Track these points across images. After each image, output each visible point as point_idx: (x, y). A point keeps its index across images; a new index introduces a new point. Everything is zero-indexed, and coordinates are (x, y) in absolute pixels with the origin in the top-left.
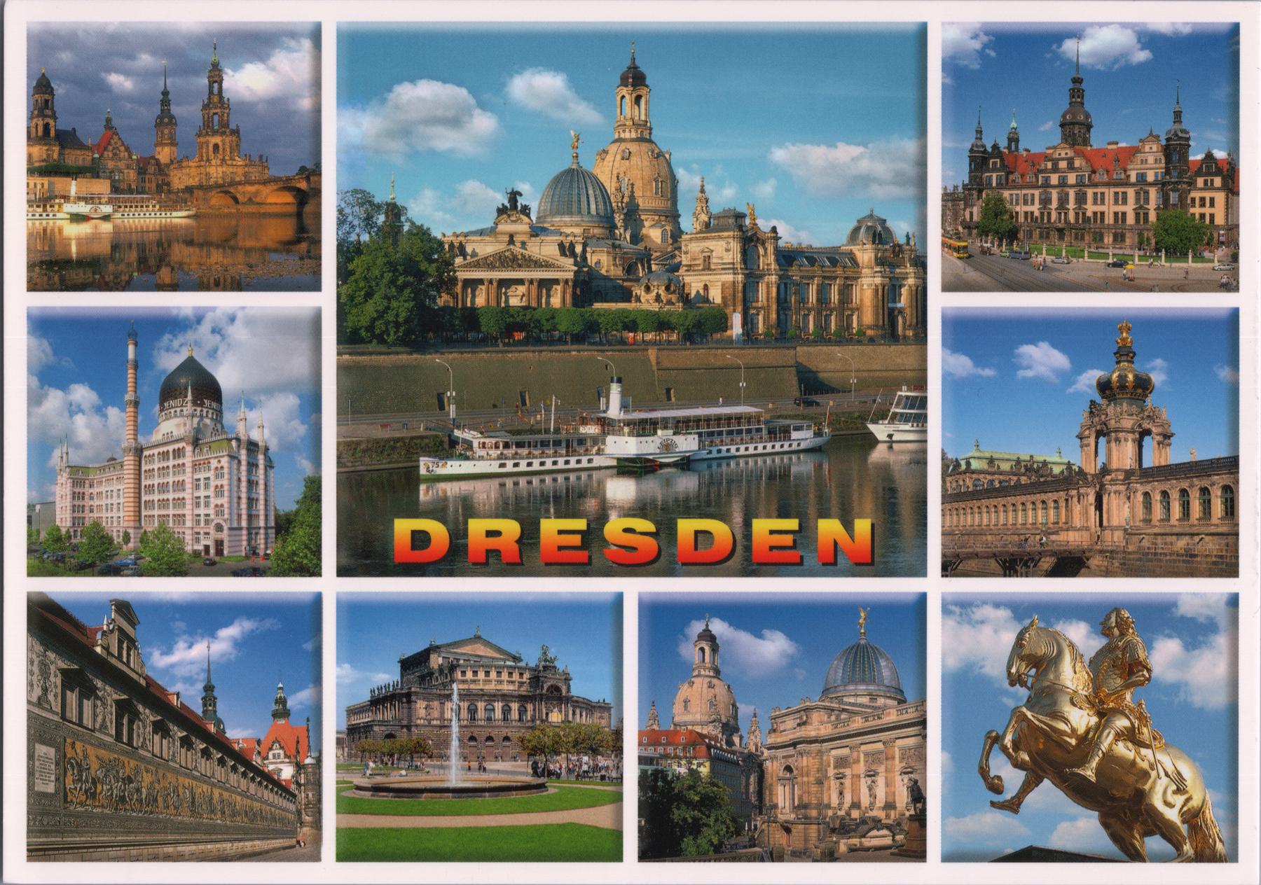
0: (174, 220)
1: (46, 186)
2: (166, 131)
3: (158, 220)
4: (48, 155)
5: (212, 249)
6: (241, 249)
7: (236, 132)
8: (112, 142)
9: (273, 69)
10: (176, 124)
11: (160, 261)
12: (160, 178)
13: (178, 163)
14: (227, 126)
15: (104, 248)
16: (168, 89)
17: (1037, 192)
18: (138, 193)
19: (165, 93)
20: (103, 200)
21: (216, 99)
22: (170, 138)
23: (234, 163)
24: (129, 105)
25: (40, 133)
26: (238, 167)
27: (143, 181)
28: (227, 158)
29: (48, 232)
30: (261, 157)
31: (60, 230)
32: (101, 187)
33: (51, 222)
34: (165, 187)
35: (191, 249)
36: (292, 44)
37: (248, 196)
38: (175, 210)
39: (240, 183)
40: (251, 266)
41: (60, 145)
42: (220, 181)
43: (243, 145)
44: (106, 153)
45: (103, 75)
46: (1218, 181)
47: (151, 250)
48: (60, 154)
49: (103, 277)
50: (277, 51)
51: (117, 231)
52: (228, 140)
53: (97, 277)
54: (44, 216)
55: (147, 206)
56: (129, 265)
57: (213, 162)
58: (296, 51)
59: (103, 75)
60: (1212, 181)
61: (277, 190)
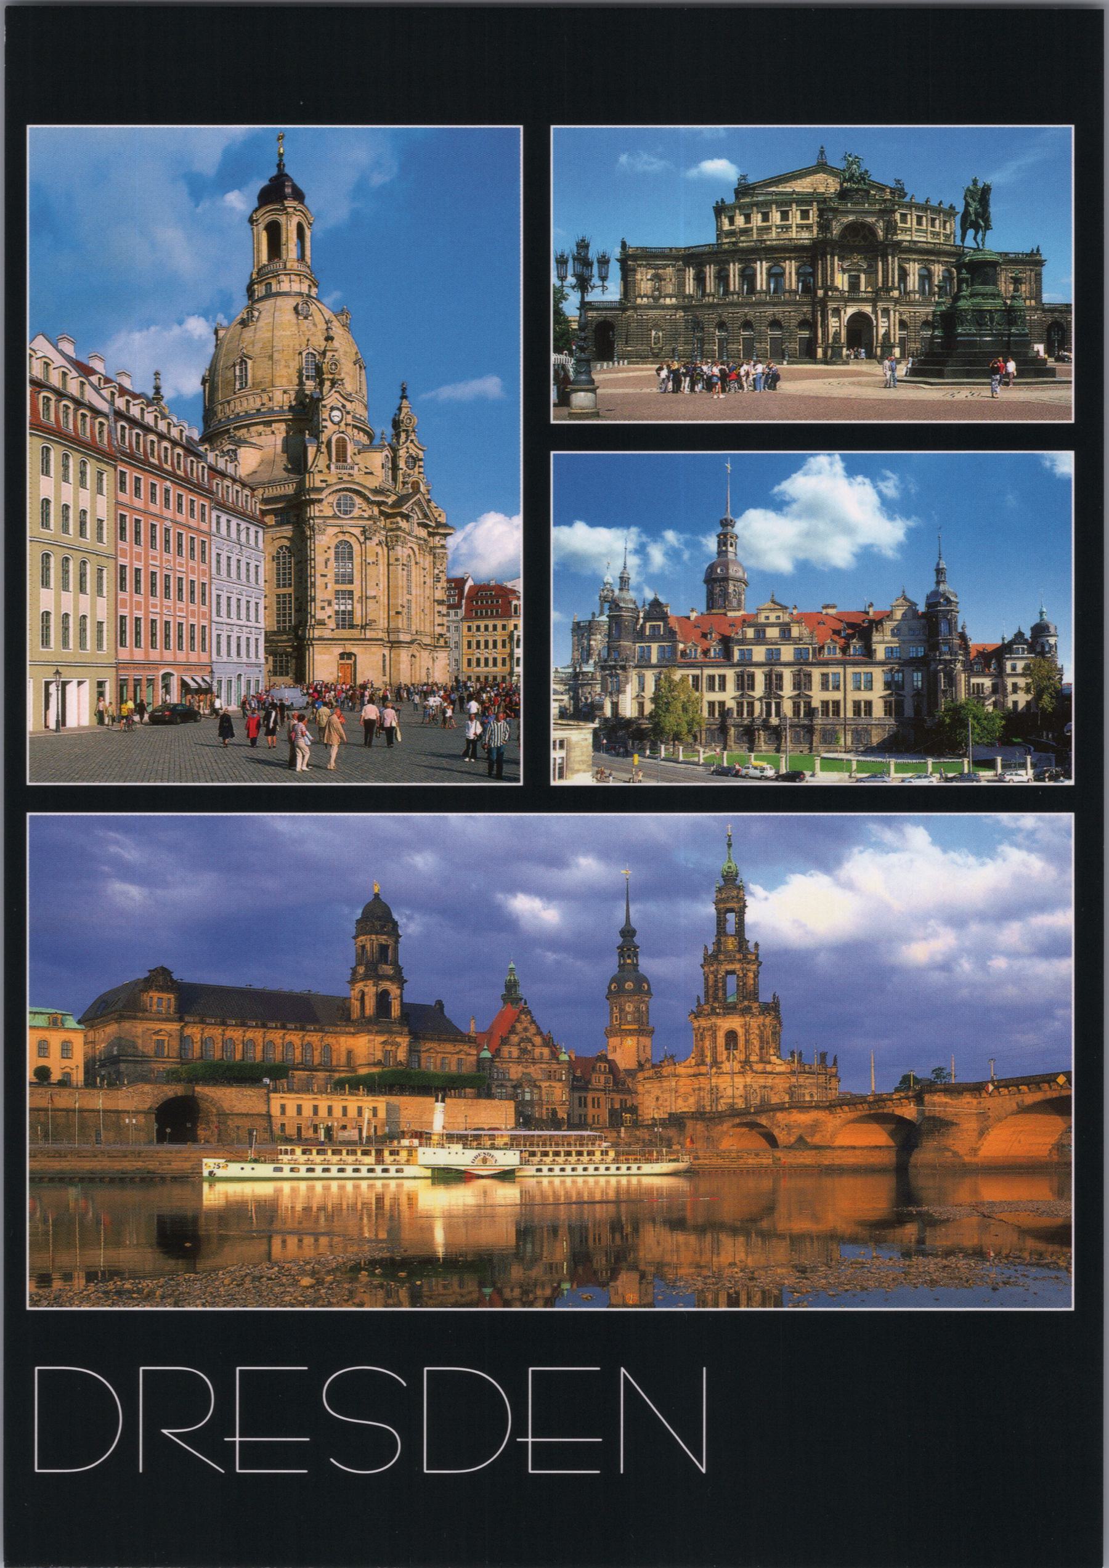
0: (646, 1181)
2: (629, 1008)
3: (613, 1180)
4: (386, 1053)
6: (781, 1237)
8: (519, 1027)
9: (849, 886)
10: (649, 993)
11: (618, 1259)
12: (617, 1097)
14: (754, 995)
16: (634, 924)
18: (571, 1127)
19: (628, 933)
20: (499, 1142)
21: (731, 944)
23: (769, 1068)
24: (551, 957)
27: (582, 1103)
28: (754, 1058)
29: (387, 1202)
30: (823, 1056)
31: (412, 1199)
33: (393, 1184)
35: (680, 1237)
36: (888, 836)
37: (797, 1132)
38: (649, 1161)
39: (780, 1108)
40: (803, 1271)
41: (411, 1033)
42: (740, 1104)
44: (505, 1049)
45: (500, 897)
48: (412, 1051)
50: (856, 850)
51: (527, 1202)
52: (754, 1022)
55: (591, 1153)
56: (551, 1267)
57: (726, 1067)
58: (895, 850)
59: (500, 897)
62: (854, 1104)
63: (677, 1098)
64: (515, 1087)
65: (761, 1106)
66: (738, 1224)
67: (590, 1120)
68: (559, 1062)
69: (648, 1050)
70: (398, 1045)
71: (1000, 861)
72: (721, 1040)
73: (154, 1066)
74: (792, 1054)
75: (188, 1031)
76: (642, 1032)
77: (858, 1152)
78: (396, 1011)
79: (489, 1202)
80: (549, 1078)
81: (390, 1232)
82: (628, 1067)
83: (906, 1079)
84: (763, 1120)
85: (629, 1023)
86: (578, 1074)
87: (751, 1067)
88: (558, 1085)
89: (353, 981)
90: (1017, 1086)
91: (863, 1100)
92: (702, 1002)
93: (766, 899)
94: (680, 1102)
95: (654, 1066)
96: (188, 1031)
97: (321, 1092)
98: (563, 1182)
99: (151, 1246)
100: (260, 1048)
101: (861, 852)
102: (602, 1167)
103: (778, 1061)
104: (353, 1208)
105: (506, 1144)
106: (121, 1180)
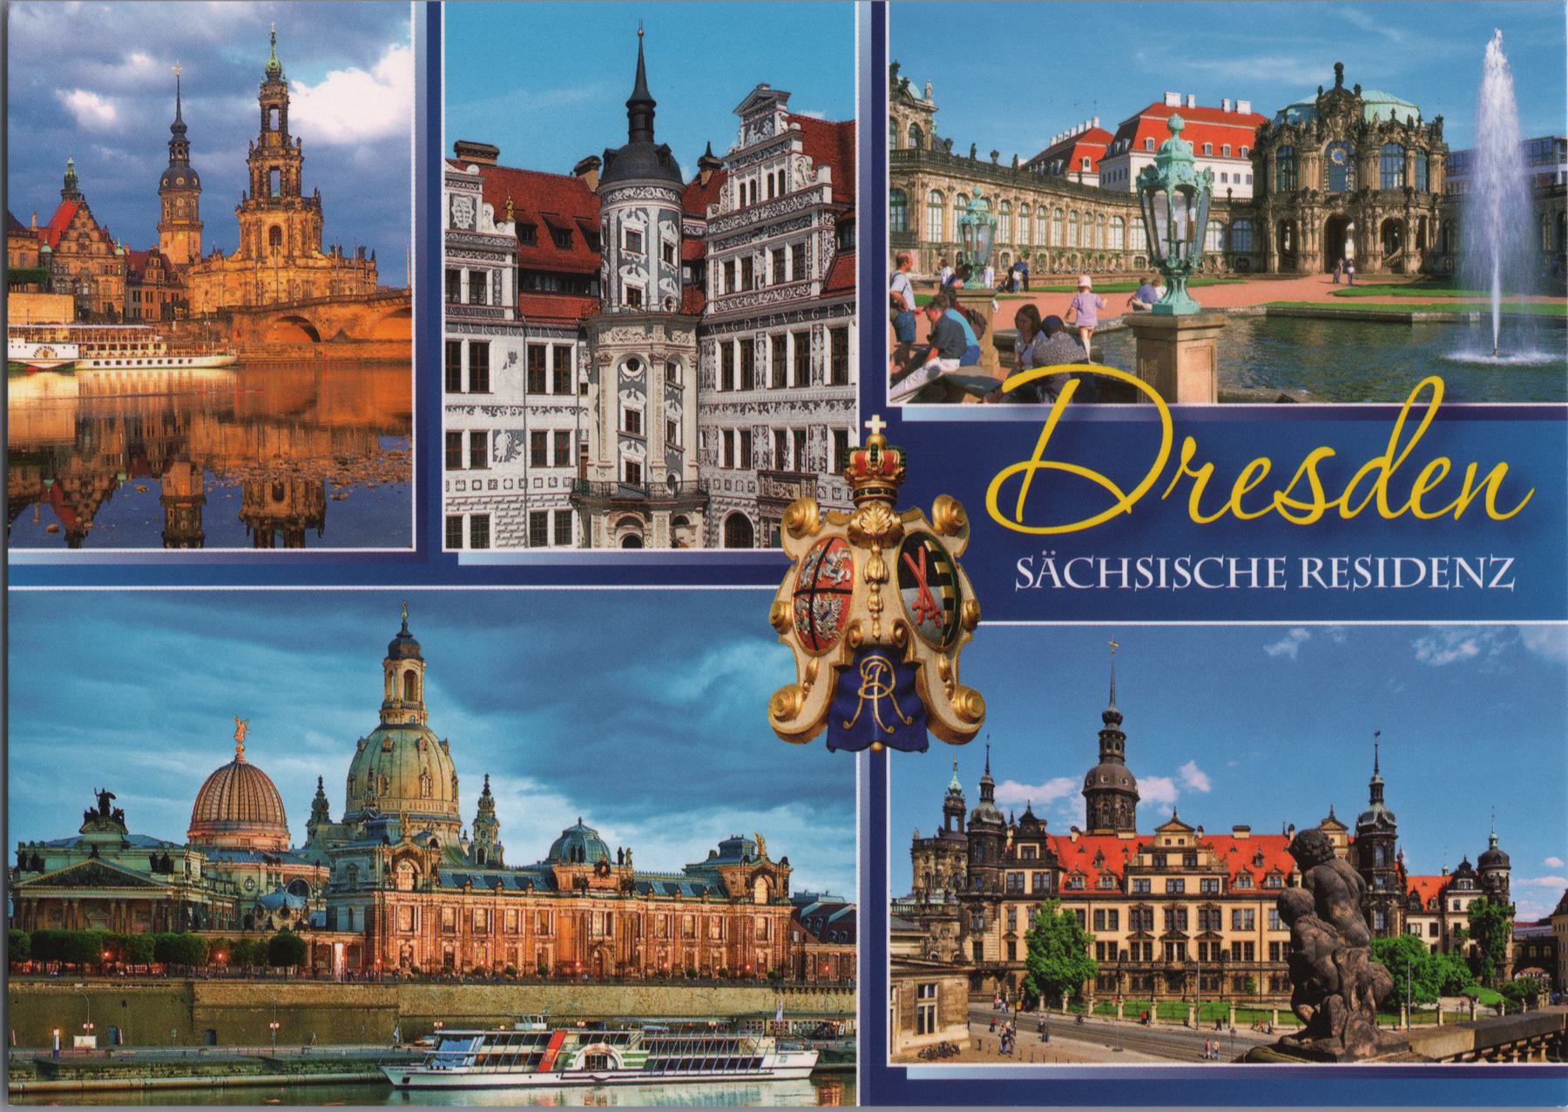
0: (197, 374)
2: (180, 202)
3: (165, 373)
5: (268, 429)
6: (323, 429)
7: (313, 204)
8: (78, 223)
9: (386, 82)
10: (198, 187)
12: (169, 292)
13: (204, 262)
15: (60, 426)
16: (185, 119)
18: (127, 321)
19: (179, 128)
20: (60, 336)
21: (275, 139)
22: (188, 216)
23: (311, 262)
24: (107, 152)
26: (316, 271)
27: (137, 297)
28: (296, 253)
30: (362, 251)
35: (228, 429)
38: (201, 355)
39: (321, 302)
42: (284, 298)
43: (327, 230)
44: (65, 245)
45: (59, 92)
47: (151, 431)
49: (59, 483)
50: (392, 46)
51: (85, 393)
52: (297, 218)
53: (49, 482)
55: (144, 347)
56: (109, 459)
57: (271, 261)
59: (59, 92)
61: (386, 317)
62: (391, 299)
63: (224, 292)
64: (74, 282)
65: (304, 300)
66: (283, 416)
67: (143, 314)
68: (115, 257)
69: (198, 245)
72: (266, 235)
74: (333, 248)
77: (395, 346)
79: (50, 395)
80: (106, 273)
82: (179, 261)
85: (180, 218)
86: (133, 268)
87: (294, 261)
88: (113, 279)
92: (248, 197)
93: (308, 95)
94: (227, 295)
95: (203, 261)
101: (396, 49)
103: (319, 256)
105: (65, 338)
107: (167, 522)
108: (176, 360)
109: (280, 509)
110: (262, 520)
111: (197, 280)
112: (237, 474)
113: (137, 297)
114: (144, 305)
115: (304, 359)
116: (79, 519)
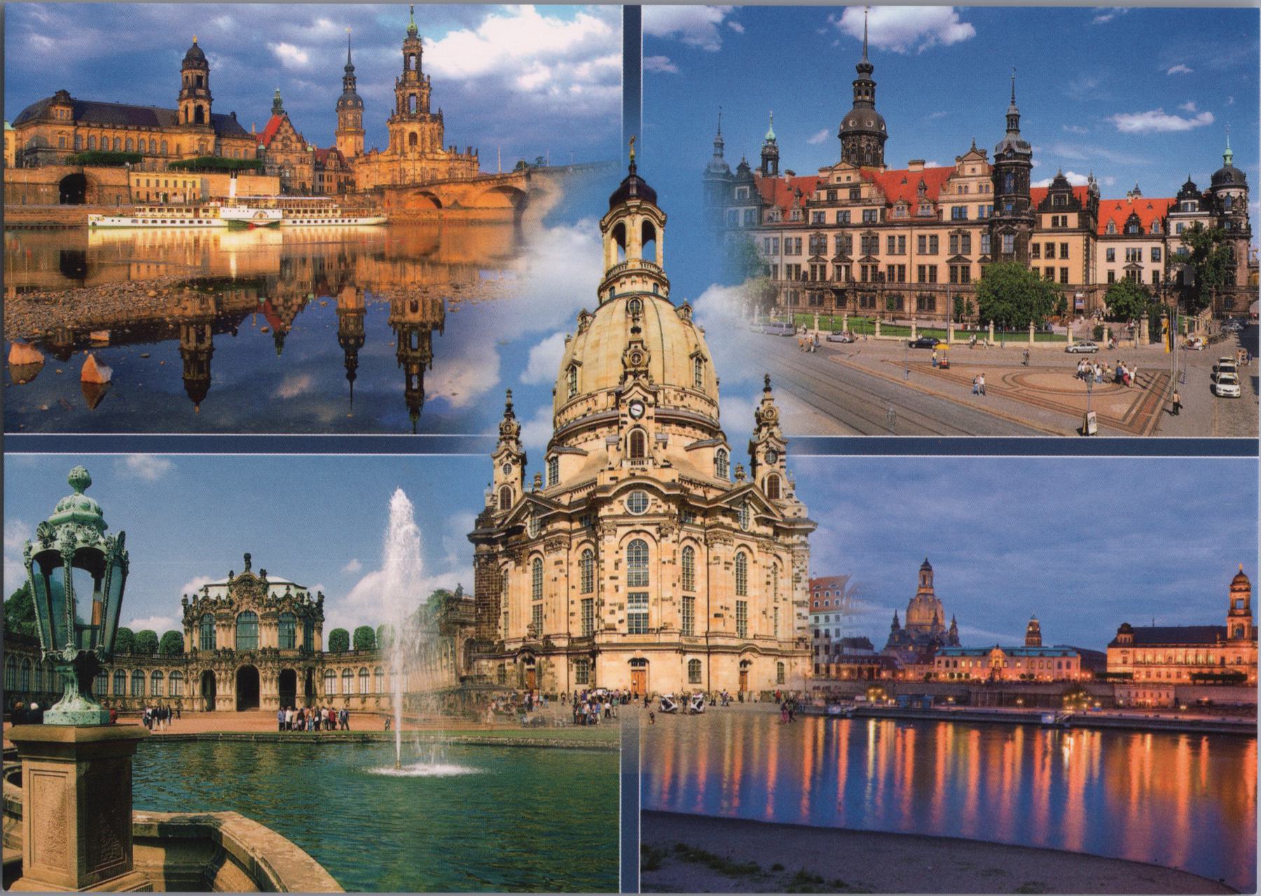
0: (361, 230)
1: (198, 185)
2: (350, 117)
3: (340, 229)
6: (443, 265)
7: (438, 118)
8: (282, 130)
9: (485, 39)
10: (362, 108)
12: (342, 175)
13: (365, 156)
14: (428, 110)
15: (271, 264)
17: (805, 236)
18: (314, 194)
19: (349, 69)
20: (270, 204)
21: (413, 76)
22: (356, 125)
23: (436, 157)
24: (302, 84)
25: (191, 118)
26: (440, 163)
27: (321, 178)
28: (427, 150)
29: (201, 242)
30: (469, 149)
31: (216, 242)
32: (268, 186)
33: (204, 230)
34: (349, 188)
38: (363, 217)
39: (442, 182)
41: (216, 133)
42: (418, 180)
43: (448, 135)
46: (1073, 220)
47: (330, 266)
48: (217, 145)
49: (269, 300)
50: (489, 16)
51: (287, 243)
52: (428, 127)
53: (263, 300)
54: (196, 223)
55: (326, 211)
56: (302, 285)
57: (410, 156)
58: (513, 16)
59: (270, 45)
60: (1064, 219)
61: (487, 191)
64: (280, 168)
66: (417, 257)
69: (362, 144)
70: (208, 141)
71: (576, 23)
72: (407, 138)
73: (59, 154)
74: (450, 147)
75: (79, 132)
76: (357, 133)
78: (207, 119)
81: (203, 261)
83: (520, 164)
84: (433, 190)
86: (319, 160)
88: (307, 167)
89: (181, 100)
90: (587, 169)
91: (493, 178)
92: (395, 113)
94: (381, 178)
95: (365, 155)
96: (79, 132)
97: (161, 172)
98: (309, 230)
99: (56, 271)
100: (123, 143)
102: (333, 220)
104: (179, 246)
106: (38, 228)
107: (340, 325)
108: (346, 220)
109: (416, 318)
110: (403, 325)
111: (361, 168)
112: (387, 296)
113: (321, 178)
114: (326, 184)
115: (431, 220)
116: (283, 324)
